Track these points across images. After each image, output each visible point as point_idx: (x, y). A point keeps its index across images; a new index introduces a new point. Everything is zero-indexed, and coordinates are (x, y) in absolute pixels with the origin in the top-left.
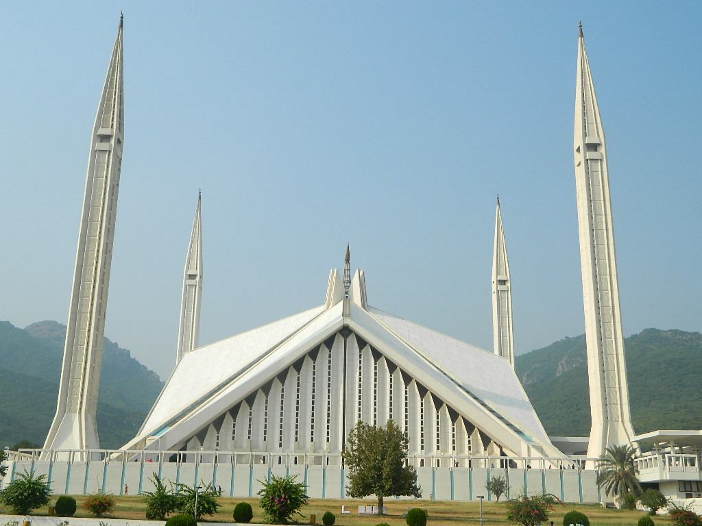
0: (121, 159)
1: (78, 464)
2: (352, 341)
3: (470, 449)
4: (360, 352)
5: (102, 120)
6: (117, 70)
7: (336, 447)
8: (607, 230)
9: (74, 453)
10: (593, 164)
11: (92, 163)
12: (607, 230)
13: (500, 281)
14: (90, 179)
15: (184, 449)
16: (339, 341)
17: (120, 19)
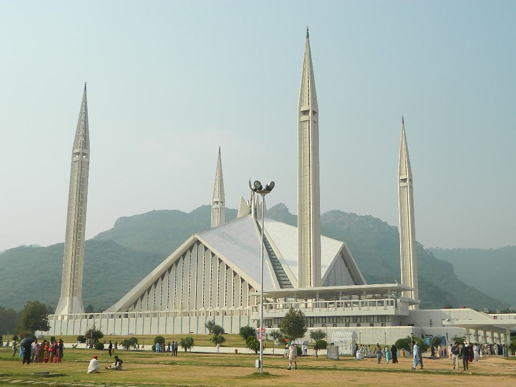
0: (89, 163)
8: (310, 166)
10: (305, 124)
11: (72, 168)
12: (310, 166)
14: (71, 177)
15: (128, 311)
16: (196, 245)
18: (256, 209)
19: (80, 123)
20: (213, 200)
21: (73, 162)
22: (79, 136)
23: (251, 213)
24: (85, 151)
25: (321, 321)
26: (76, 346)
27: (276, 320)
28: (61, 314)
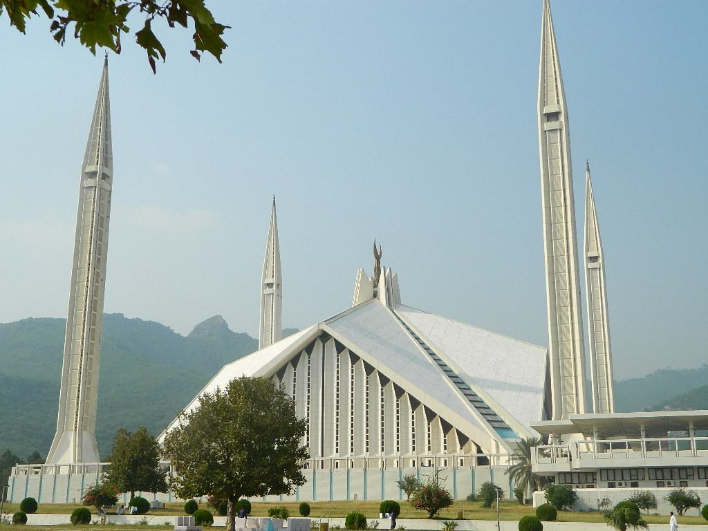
0: (110, 192)
1: (62, 476)
2: (331, 345)
3: (445, 449)
4: (338, 356)
5: (88, 160)
6: (102, 109)
7: (318, 453)
8: (565, 206)
9: (59, 467)
11: (81, 200)
12: (565, 206)
13: (591, 258)
14: (80, 214)
16: (319, 345)
17: (105, 58)
18: (388, 290)
19: (97, 121)
20: (264, 279)
21: (83, 188)
22: (94, 146)
23: (375, 295)
24: (106, 171)
25: (702, 475)
26: (456, 525)
27: (604, 473)
28: (58, 464)
